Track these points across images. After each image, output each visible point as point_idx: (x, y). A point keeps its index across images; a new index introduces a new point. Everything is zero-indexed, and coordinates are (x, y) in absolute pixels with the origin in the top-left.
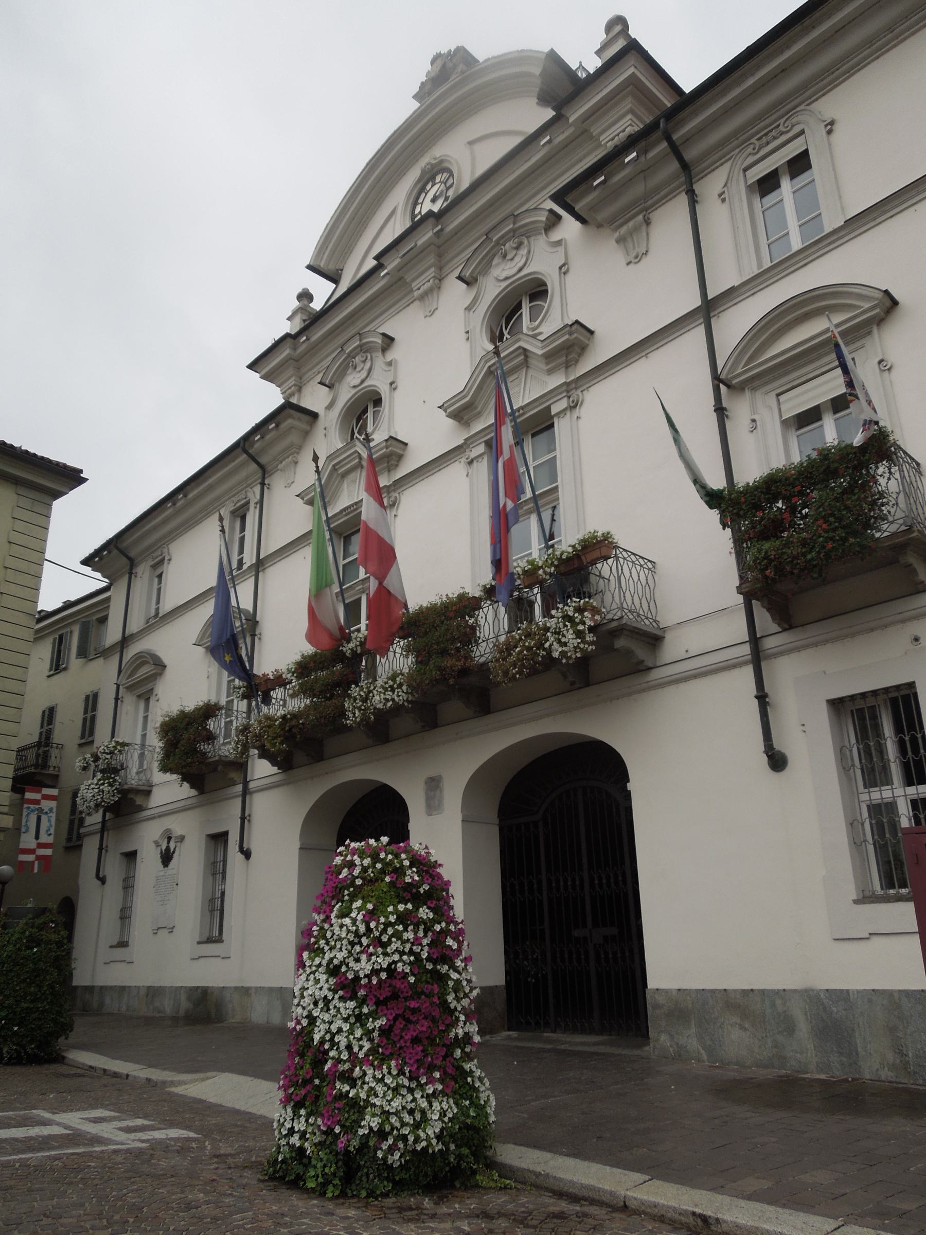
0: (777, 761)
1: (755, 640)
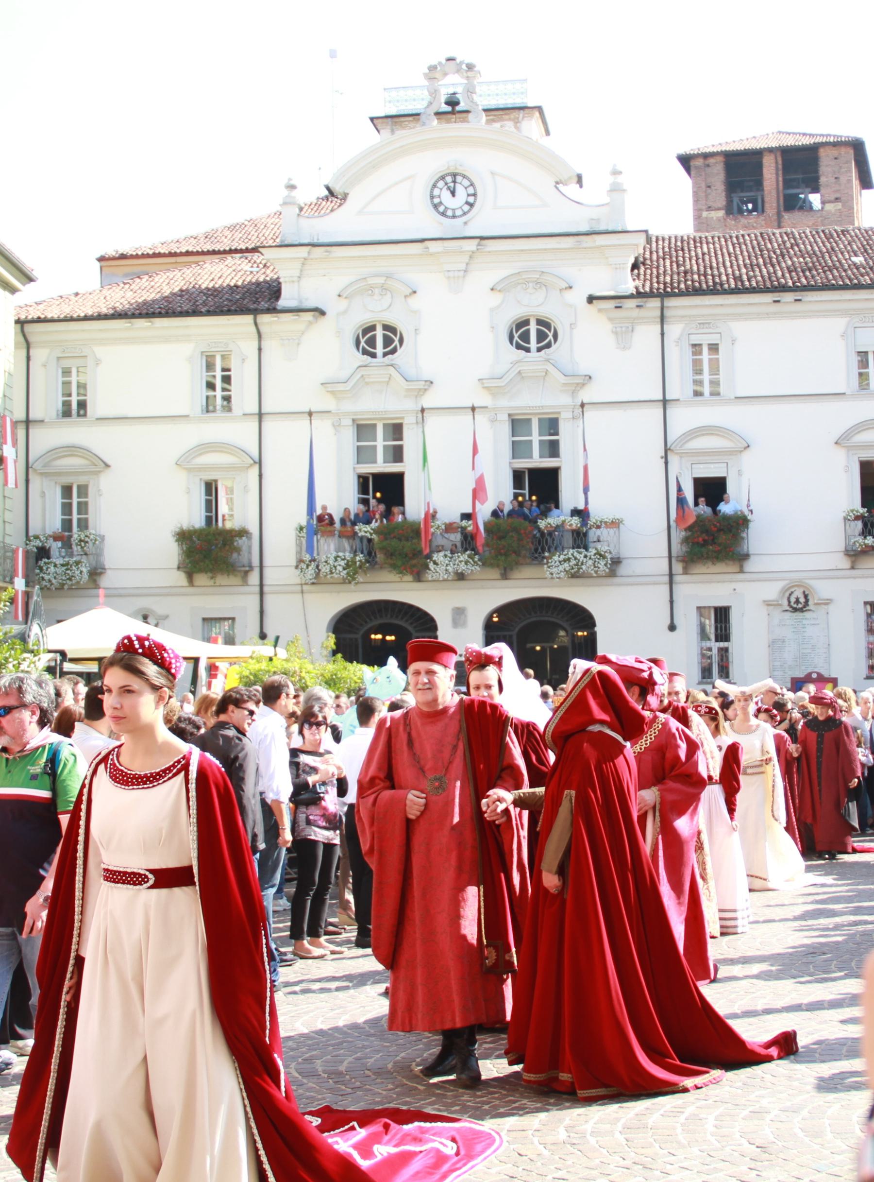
0: (672, 628)
1: (671, 575)
